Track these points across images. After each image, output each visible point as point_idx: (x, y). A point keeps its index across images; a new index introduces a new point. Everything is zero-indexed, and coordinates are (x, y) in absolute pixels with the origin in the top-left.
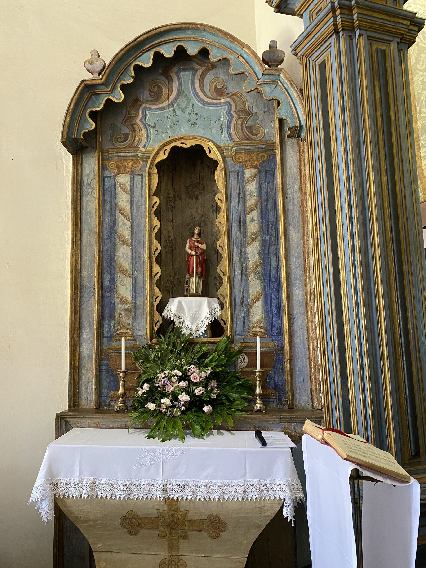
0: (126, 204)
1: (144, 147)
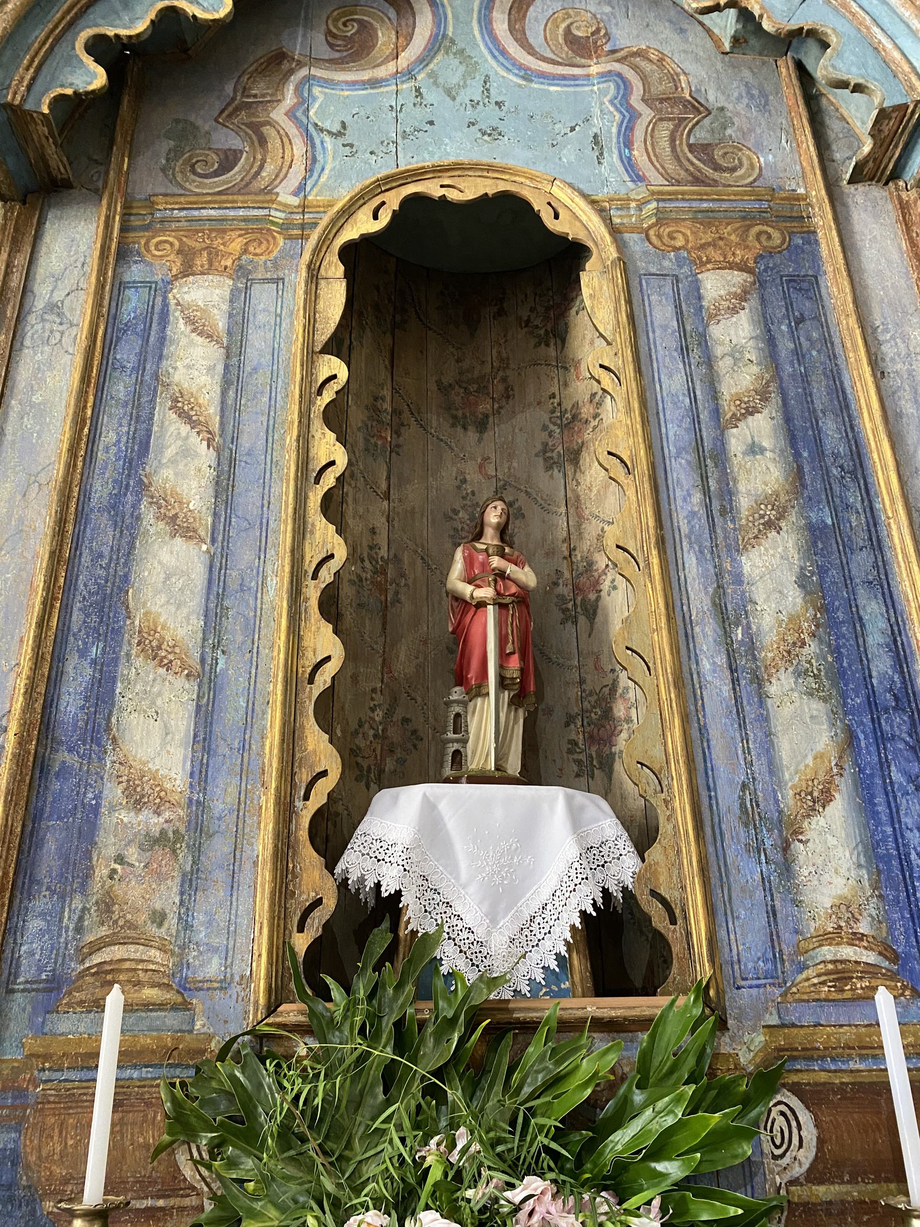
0: (204, 379)
1: (295, 194)
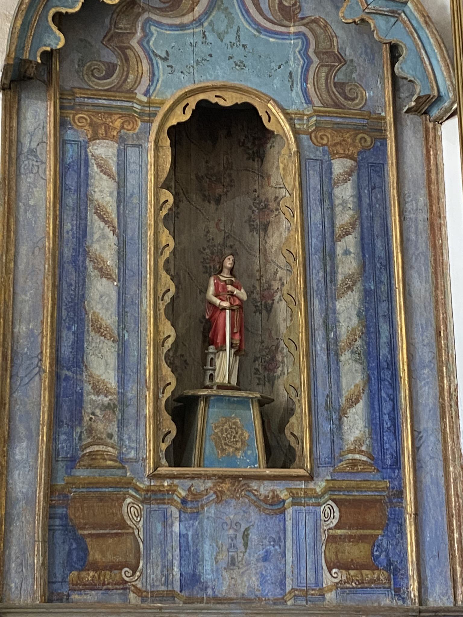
0: (108, 199)
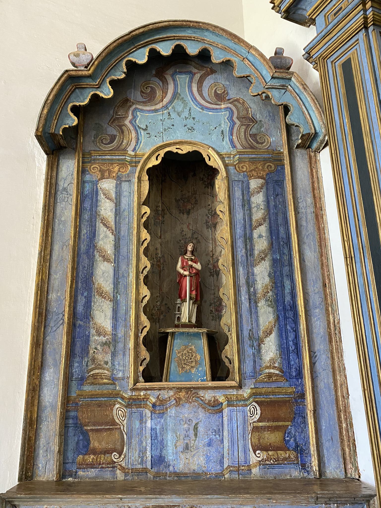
0: (110, 213)
1: (133, 151)
